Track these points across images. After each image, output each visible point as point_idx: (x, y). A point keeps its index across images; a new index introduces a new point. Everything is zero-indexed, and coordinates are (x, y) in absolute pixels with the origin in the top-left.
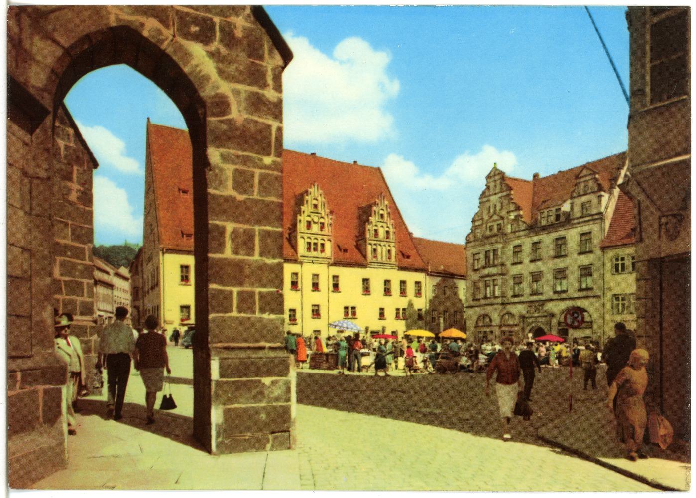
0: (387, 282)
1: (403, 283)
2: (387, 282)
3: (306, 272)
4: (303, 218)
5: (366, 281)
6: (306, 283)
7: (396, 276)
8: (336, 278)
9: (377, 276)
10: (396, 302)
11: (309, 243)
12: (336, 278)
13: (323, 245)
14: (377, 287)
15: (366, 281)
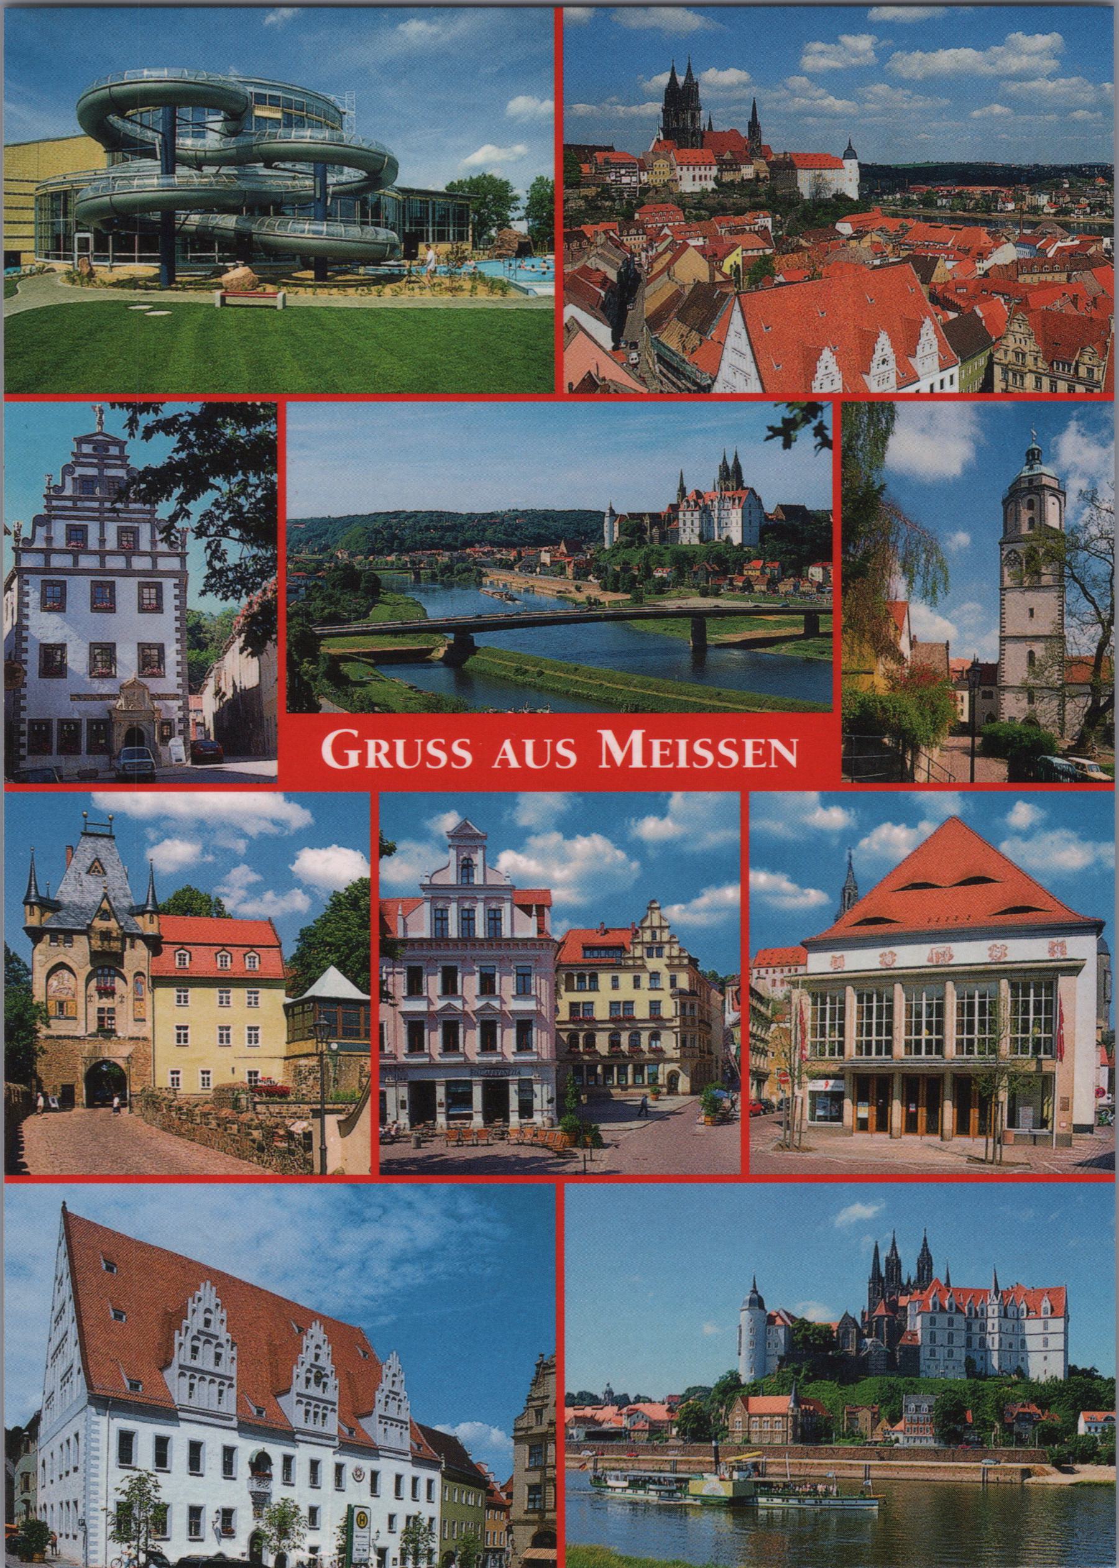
0: (399, 1478)
1: (415, 1480)
2: (399, 1478)
3: (303, 1454)
4: (300, 1371)
5: (375, 1475)
6: (301, 1471)
7: (408, 1470)
8: (339, 1468)
9: (388, 1468)
10: (406, 1508)
11: (307, 1412)
12: (339, 1468)
13: (324, 1416)
14: (386, 1484)
15: (375, 1475)
